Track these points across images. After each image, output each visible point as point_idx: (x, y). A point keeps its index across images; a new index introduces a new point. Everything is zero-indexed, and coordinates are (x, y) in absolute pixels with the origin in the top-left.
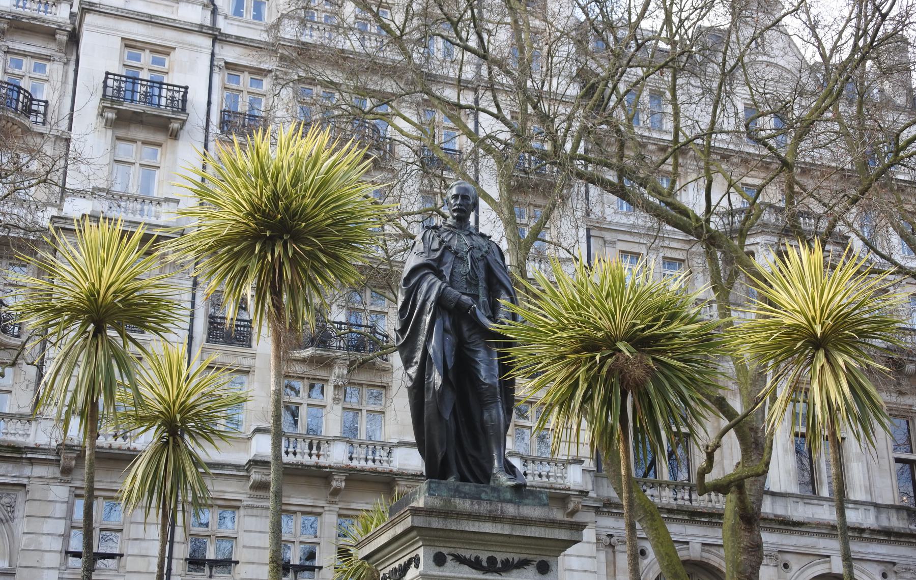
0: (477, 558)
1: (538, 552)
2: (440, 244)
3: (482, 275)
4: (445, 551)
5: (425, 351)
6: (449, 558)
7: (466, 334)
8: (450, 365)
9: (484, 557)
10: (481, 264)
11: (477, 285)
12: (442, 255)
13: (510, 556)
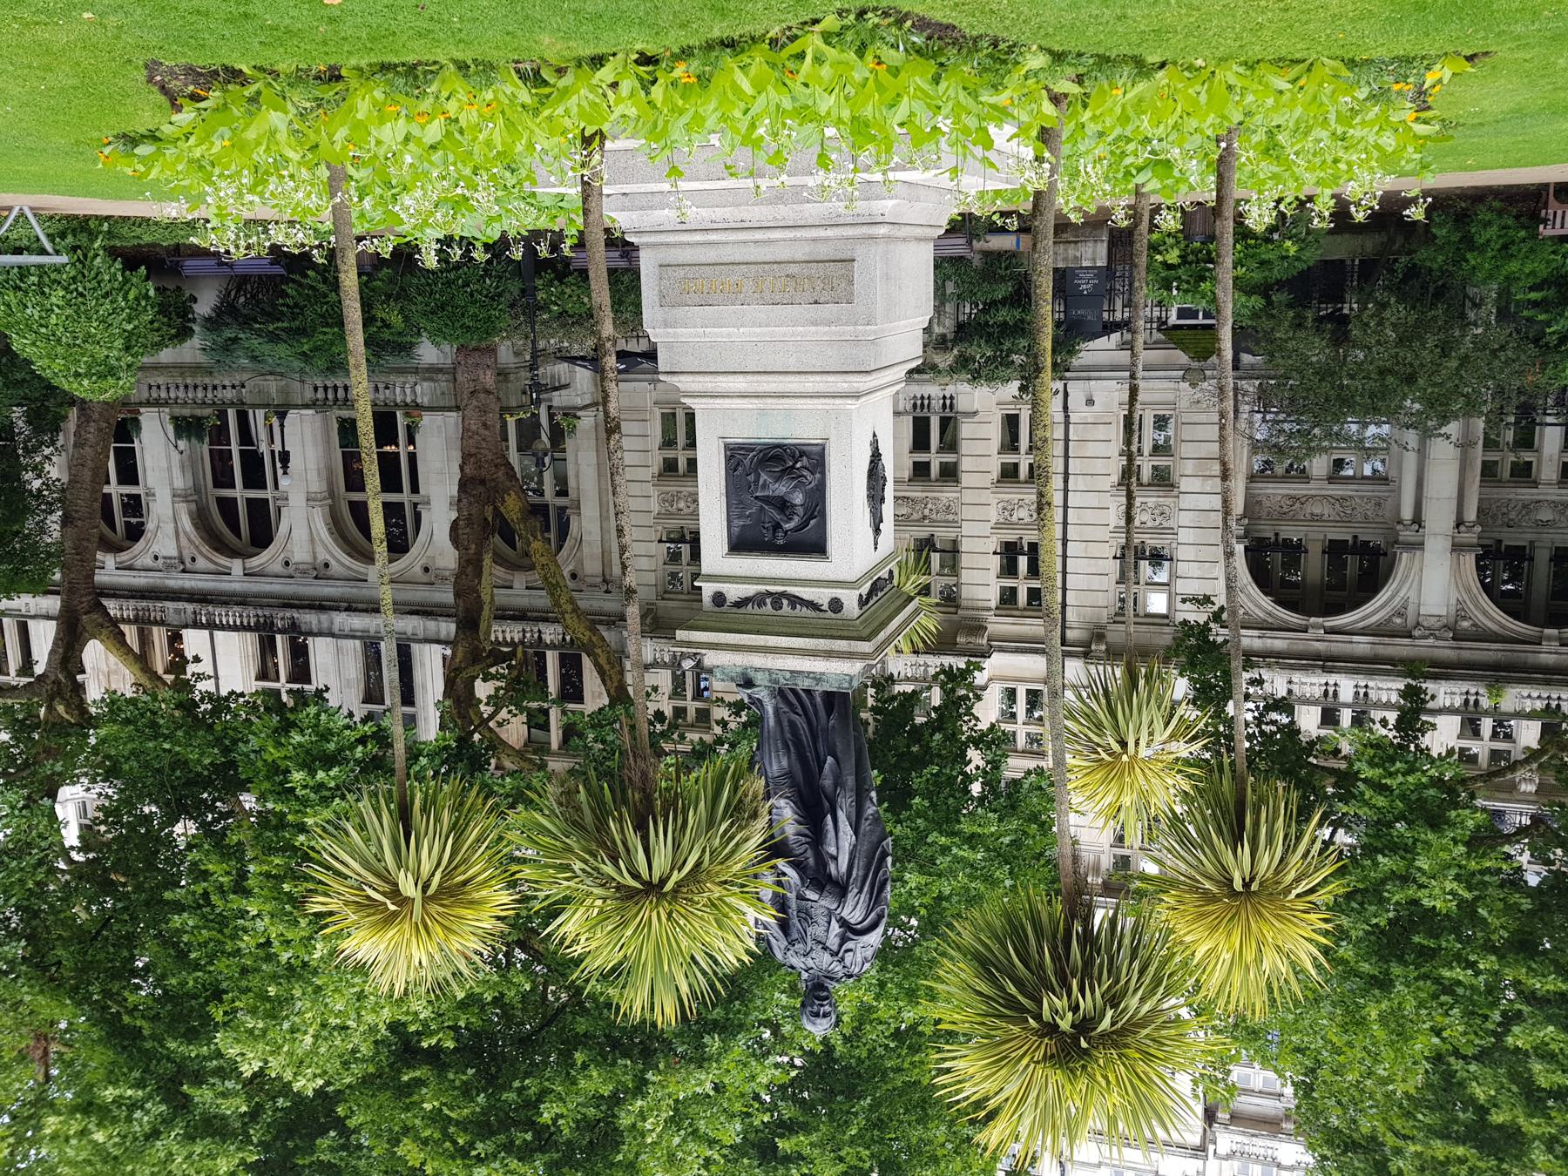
0: (794, 608)
2: (843, 959)
4: (830, 614)
5: (856, 833)
6: (825, 607)
7: (809, 853)
10: (795, 936)
12: (841, 946)
13: (757, 610)
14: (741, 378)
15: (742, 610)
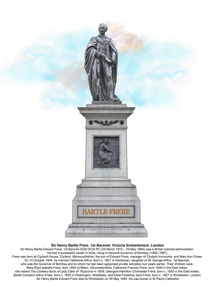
3: (108, 49)
5: (92, 69)
8: (98, 72)
9: (104, 121)
10: (108, 45)
11: (106, 51)
13: (112, 120)
14: (115, 186)
15: (116, 120)
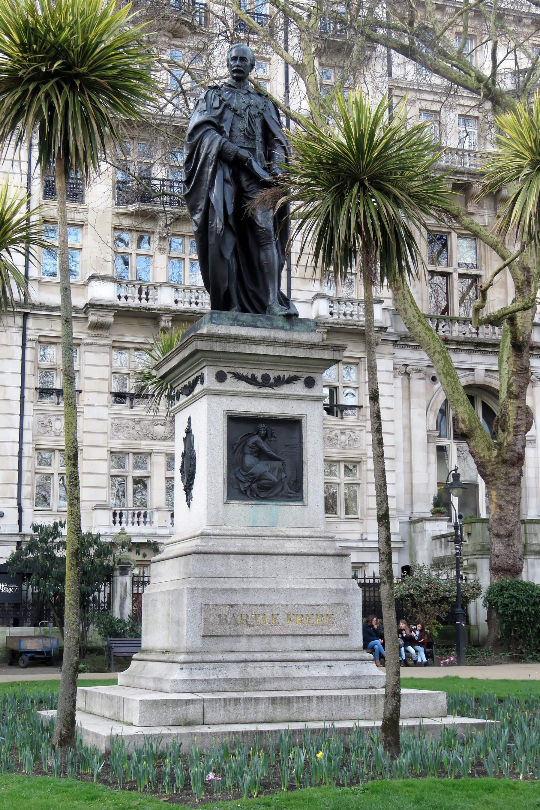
0: (253, 376)
1: (306, 370)
4: (226, 370)
6: (229, 376)
9: (259, 375)
15: (292, 374)
